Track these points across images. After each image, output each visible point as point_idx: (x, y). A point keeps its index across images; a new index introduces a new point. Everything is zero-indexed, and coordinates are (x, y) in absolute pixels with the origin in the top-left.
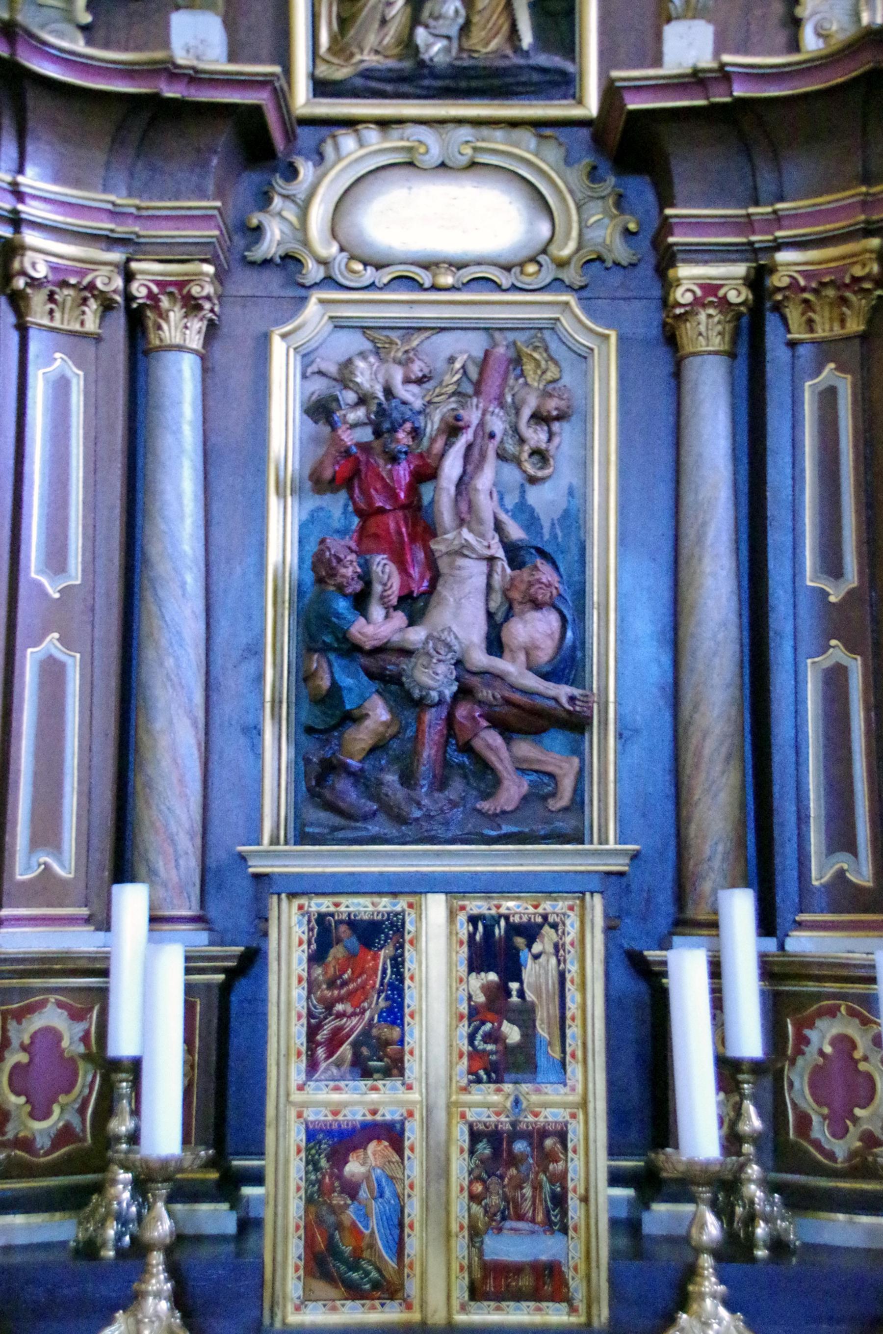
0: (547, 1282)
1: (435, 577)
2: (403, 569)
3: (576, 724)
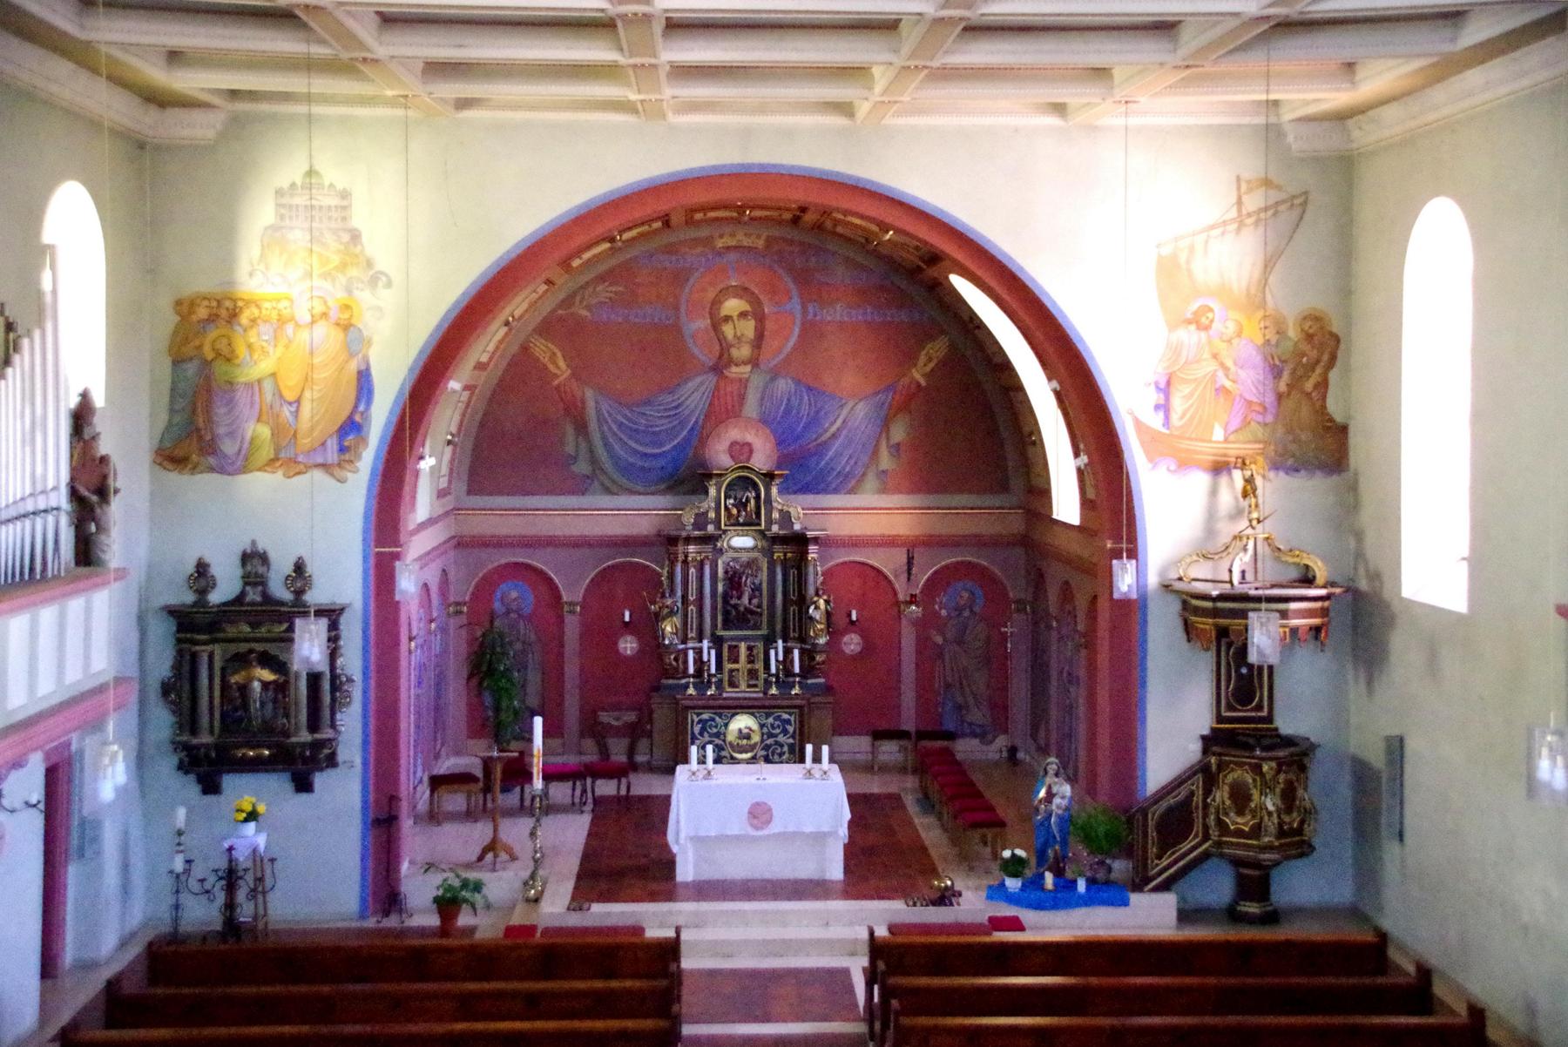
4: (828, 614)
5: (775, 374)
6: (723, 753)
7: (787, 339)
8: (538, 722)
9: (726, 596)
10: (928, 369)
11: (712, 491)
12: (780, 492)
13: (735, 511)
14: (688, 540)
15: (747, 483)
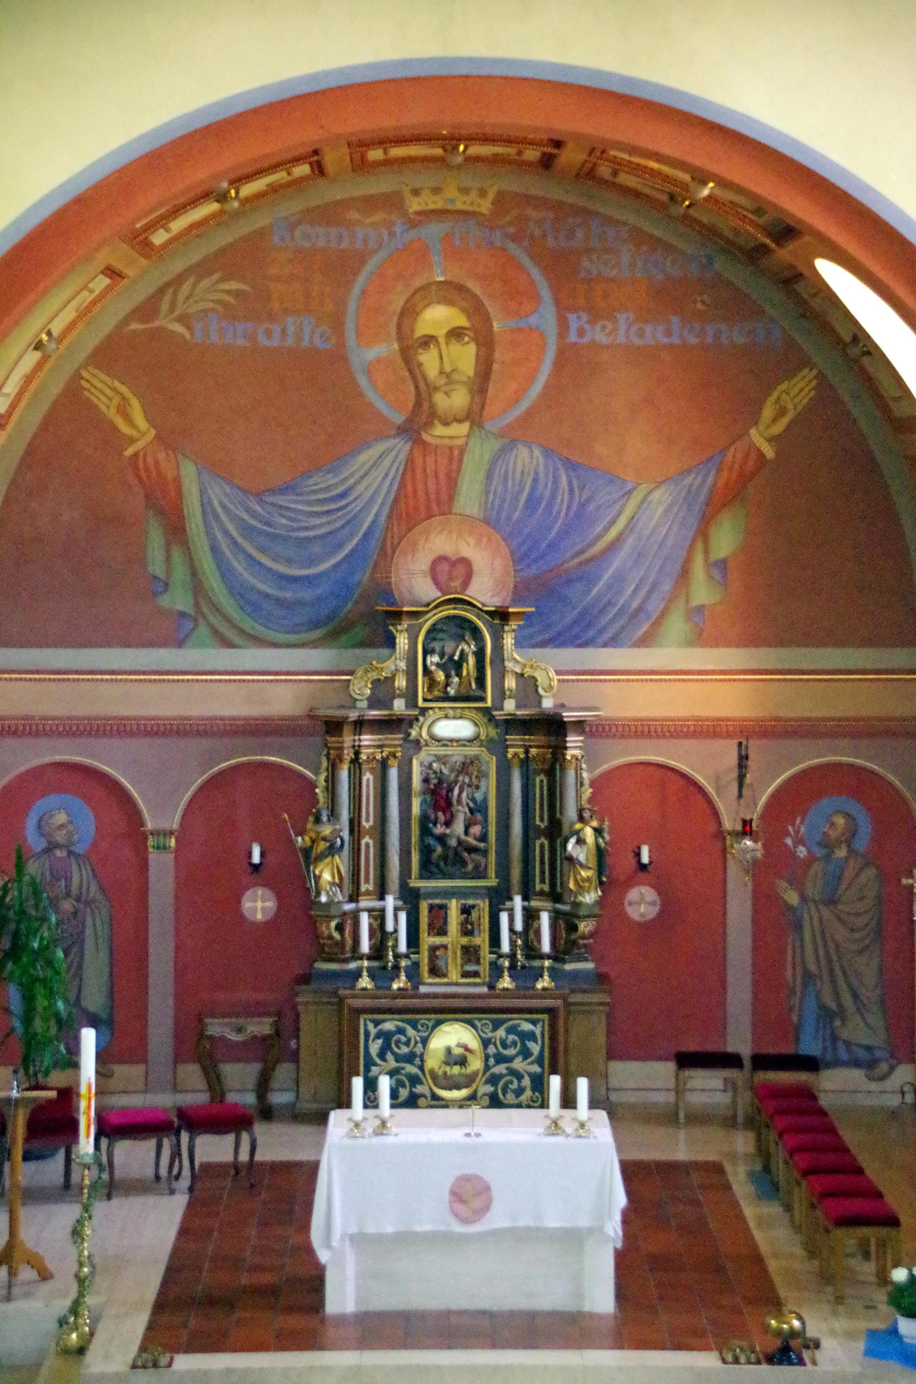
0: (476, 974)
1: (452, 816)
2: (444, 814)
3: (485, 853)
4: (600, 853)
5: (511, 438)
6: (419, 1089)
7: (531, 379)
8: (89, 1037)
9: (424, 820)
10: (778, 428)
11: (402, 641)
12: (518, 644)
13: (441, 676)
14: (360, 725)
15: (463, 628)
